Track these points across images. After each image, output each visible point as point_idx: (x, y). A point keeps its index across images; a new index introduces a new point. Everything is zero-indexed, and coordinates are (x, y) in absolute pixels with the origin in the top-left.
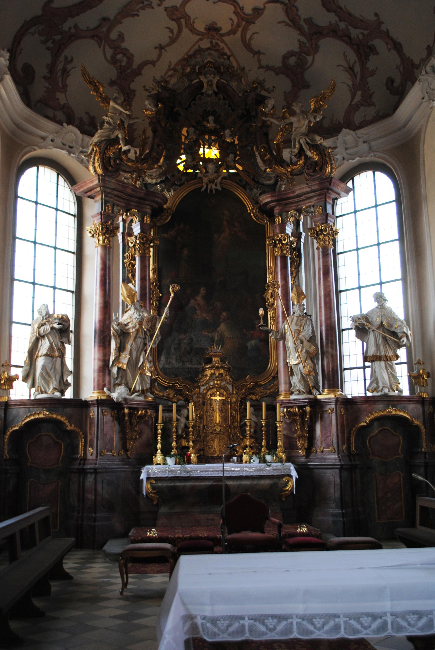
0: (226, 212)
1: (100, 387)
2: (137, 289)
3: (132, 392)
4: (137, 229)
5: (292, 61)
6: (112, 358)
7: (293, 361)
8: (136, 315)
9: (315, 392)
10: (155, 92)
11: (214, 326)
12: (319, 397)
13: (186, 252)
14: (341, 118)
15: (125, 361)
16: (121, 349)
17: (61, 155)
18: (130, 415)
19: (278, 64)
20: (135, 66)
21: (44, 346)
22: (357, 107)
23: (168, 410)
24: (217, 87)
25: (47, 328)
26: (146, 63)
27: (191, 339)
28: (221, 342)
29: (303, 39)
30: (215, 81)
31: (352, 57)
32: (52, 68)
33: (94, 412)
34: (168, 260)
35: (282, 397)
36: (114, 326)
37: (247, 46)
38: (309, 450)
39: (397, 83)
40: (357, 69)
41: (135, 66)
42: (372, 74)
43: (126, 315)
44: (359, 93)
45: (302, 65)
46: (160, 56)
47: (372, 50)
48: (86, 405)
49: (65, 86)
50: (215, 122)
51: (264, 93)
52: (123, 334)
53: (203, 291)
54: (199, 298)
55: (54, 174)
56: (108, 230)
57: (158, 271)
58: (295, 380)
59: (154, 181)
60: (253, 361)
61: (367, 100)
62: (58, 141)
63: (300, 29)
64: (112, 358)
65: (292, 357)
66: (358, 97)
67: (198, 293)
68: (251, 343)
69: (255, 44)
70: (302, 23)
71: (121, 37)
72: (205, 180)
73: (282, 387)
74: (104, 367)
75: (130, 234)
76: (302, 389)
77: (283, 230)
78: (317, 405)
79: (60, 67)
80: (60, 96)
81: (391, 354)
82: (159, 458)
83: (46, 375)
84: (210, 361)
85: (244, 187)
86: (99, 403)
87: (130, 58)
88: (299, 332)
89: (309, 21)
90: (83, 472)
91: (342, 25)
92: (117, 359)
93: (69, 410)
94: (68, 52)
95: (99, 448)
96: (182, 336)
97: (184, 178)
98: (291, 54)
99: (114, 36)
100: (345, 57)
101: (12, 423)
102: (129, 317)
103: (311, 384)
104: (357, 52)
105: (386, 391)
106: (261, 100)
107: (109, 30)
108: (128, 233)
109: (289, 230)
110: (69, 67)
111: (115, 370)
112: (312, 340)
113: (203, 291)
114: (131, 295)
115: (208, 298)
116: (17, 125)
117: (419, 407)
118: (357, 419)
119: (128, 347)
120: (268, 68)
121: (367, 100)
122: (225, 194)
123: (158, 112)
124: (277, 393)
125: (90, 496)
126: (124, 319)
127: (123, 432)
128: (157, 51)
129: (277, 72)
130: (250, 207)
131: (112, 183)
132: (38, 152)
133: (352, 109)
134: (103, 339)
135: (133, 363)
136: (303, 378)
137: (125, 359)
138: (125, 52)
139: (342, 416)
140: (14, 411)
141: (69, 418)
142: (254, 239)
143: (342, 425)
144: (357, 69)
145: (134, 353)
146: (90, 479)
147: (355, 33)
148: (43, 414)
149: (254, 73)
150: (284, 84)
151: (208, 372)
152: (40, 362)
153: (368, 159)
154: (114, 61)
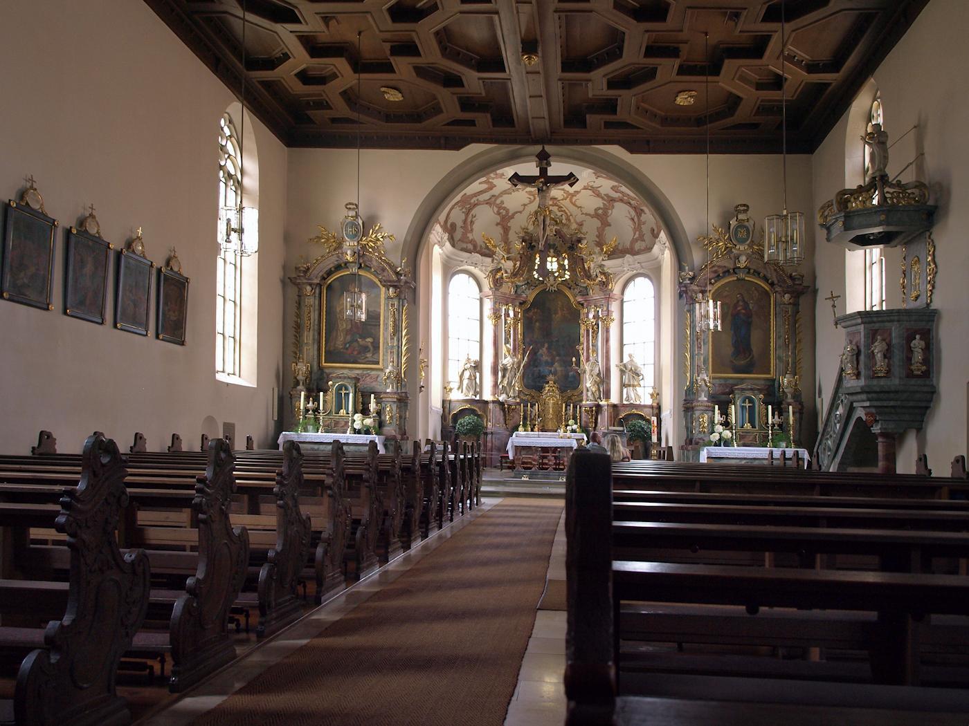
0: (560, 303)
1: (494, 394)
2: (512, 348)
3: (509, 397)
4: (511, 313)
5: (600, 212)
6: (499, 381)
7: (588, 385)
8: (511, 360)
9: (599, 400)
10: (521, 235)
11: (552, 364)
12: (600, 403)
13: (537, 324)
14: (628, 244)
15: (506, 382)
16: (504, 376)
17: (472, 269)
18: (508, 408)
19: (592, 212)
20: (510, 214)
21: (467, 374)
22: (637, 240)
23: (526, 406)
24: (556, 232)
25: (468, 365)
26: (516, 213)
27: (540, 370)
28: (555, 374)
29: (605, 202)
30: (554, 229)
31: (633, 213)
32: (465, 222)
33: (491, 406)
34: (528, 326)
35: (584, 402)
36: (500, 366)
37: (574, 204)
38: (595, 428)
39: (655, 232)
40: (636, 219)
41: (510, 214)
42: (644, 223)
43: (507, 360)
44: (637, 233)
45: (605, 214)
46: (524, 209)
47: (642, 210)
48: (487, 402)
49: (472, 230)
50: (554, 252)
51: (583, 236)
52: (505, 370)
53: (546, 345)
54: (544, 349)
55: (467, 276)
56: (496, 315)
57: (524, 334)
58: (589, 394)
59: (521, 284)
60: (570, 383)
61: (641, 238)
62: (469, 262)
63: (602, 198)
64: (499, 381)
65: (588, 383)
66: (637, 235)
67: (544, 346)
68: (571, 373)
69: (578, 203)
70: (603, 195)
71: (502, 202)
72: (549, 285)
73: (584, 397)
74: (496, 385)
75: (508, 316)
76: (592, 399)
77: (587, 317)
78: (599, 407)
79: (469, 220)
80: (469, 235)
81: (636, 383)
82: (521, 428)
83: (468, 388)
84: (548, 383)
85: (570, 288)
86: (493, 402)
87: (507, 211)
88: (592, 371)
89: (607, 195)
90: (486, 434)
91: (625, 198)
92: (502, 382)
93: (479, 405)
94: (473, 212)
95: (493, 423)
96: (535, 369)
97: (537, 282)
98: (599, 208)
99: (498, 202)
100: (629, 213)
101: (454, 409)
102: (507, 361)
103: (597, 397)
104: (635, 211)
105: (632, 402)
106: (579, 241)
107: (495, 201)
108: (507, 315)
109: (591, 316)
110: (474, 219)
111: (501, 387)
112: (599, 375)
113: (546, 345)
114: (508, 351)
115: (548, 349)
116: (448, 257)
117: (651, 410)
118: (618, 415)
119: (507, 376)
120: (586, 214)
121: (641, 238)
122: (559, 292)
123: (523, 247)
124: (582, 401)
125: (489, 444)
126: (505, 362)
127: (505, 415)
128: (523, 207)
129: (592, 217)
130: (572, 300)
131: (498, 293)
132: (459, 268)
133: (634, 241)
134: (495, 371)
135: (509, 384)
136: (593, 393)
137: (505, 383)
138: (505, 208)
139: (611, 413)
140: (453, 405)
141: (479, 409)
142: (574, 316)
143: (611, 417)
144: (636, 219)
145: (510, 379)
146: (490, 436)
147: (632, 202)
148: (468, 406)
149: (580, 218)
150: (597, 223)
151: (547, 388)
152: (466, 382)
153: (641, 271)
154: (499, 213)
